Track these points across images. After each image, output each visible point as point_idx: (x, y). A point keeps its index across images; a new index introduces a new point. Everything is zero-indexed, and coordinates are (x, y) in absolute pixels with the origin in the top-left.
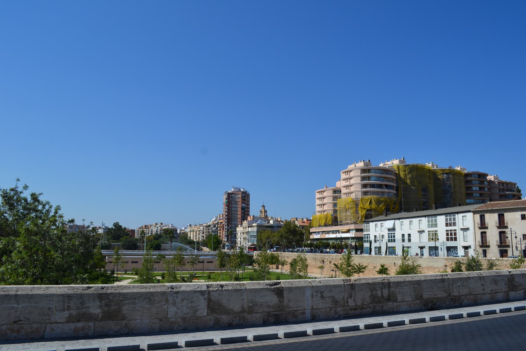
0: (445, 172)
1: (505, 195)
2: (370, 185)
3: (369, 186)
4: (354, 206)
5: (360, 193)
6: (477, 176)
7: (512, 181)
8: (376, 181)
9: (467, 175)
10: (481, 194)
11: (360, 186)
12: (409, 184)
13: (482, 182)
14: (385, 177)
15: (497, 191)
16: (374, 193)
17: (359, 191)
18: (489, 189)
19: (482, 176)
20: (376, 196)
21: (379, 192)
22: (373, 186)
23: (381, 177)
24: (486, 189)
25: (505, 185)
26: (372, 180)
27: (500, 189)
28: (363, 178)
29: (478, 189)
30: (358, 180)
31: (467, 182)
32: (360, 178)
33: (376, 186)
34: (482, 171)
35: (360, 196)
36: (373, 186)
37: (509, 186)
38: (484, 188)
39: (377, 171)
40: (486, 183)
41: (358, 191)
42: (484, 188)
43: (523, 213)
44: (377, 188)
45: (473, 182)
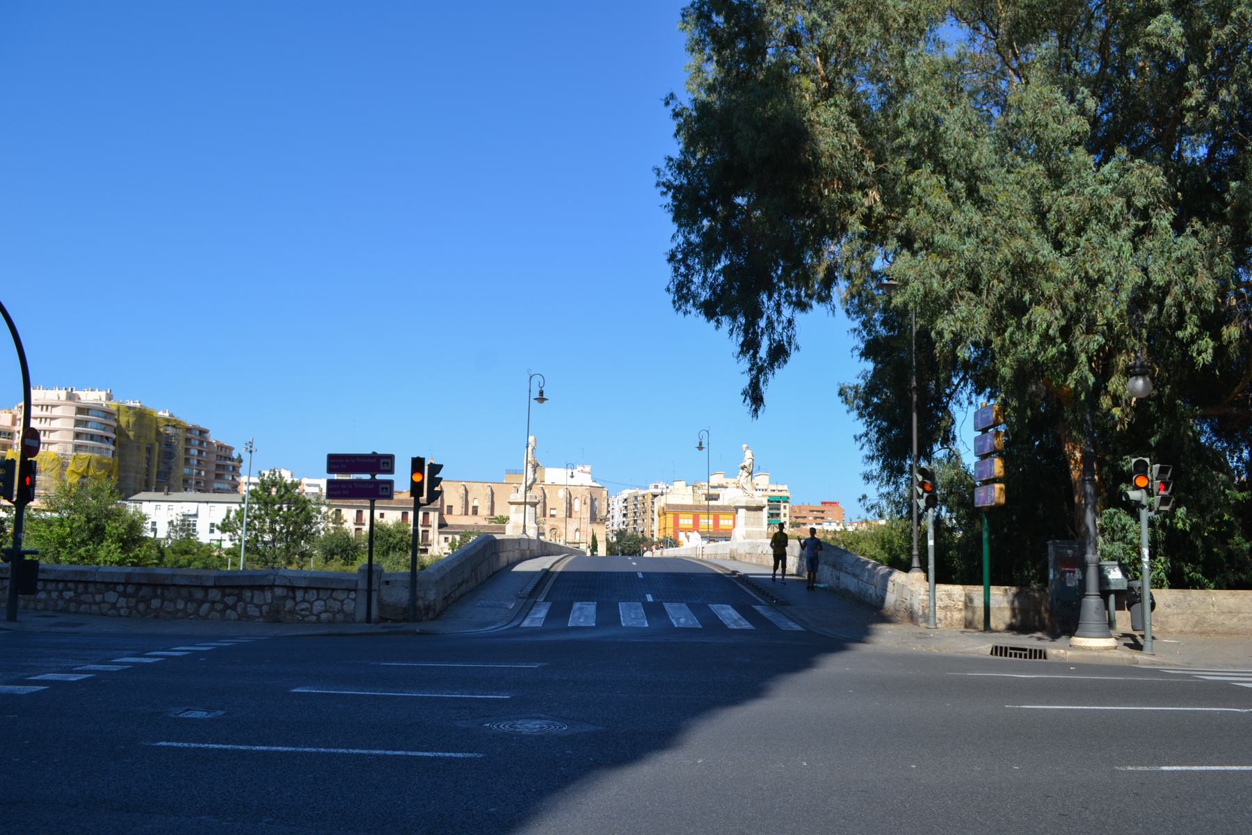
0: (170, 424)
1: (224, 466)
2: (87, 434)
3: (85, 436)
4: (59, 466)
5: (70, 448)
6: (198, 433)
7: (231, 445)
8: (97, 429)
9: (189, 430)
10: (198, 461)
11: (72, 435)
12: (132, 438)
13: (201, 443)
14: (107, 425)
15: (213, 458)
16: (93, 449)
17: (69, 443)
18: (207, 453)
19: (203, 432)
20: (97, 455)
21: (101, 448)
22: (92, 437)
23: (102, 424)
24: (204, 454)
25: (223, 450)
26: (91, 428)
27: (217, 456)
28: (78, 423)
29: (196, 452)
30: (70, 424)
31: (188, 440)
32: (72, 422)
33: (95, 438)
34: (203, 426)
35: (70, 450)
36: (92, 437)
37: (228, 451)
38: (202, 451)
39: (100, 414)
40: (205, 444)
41: (66, 443)
42: (202, 451)
43: (382, 511)
44: (96, 441)
45: (193, 442)
